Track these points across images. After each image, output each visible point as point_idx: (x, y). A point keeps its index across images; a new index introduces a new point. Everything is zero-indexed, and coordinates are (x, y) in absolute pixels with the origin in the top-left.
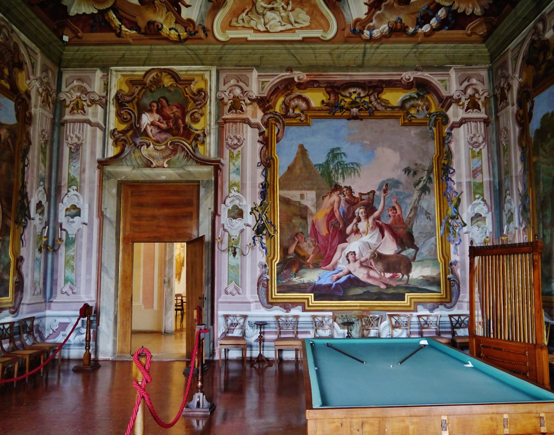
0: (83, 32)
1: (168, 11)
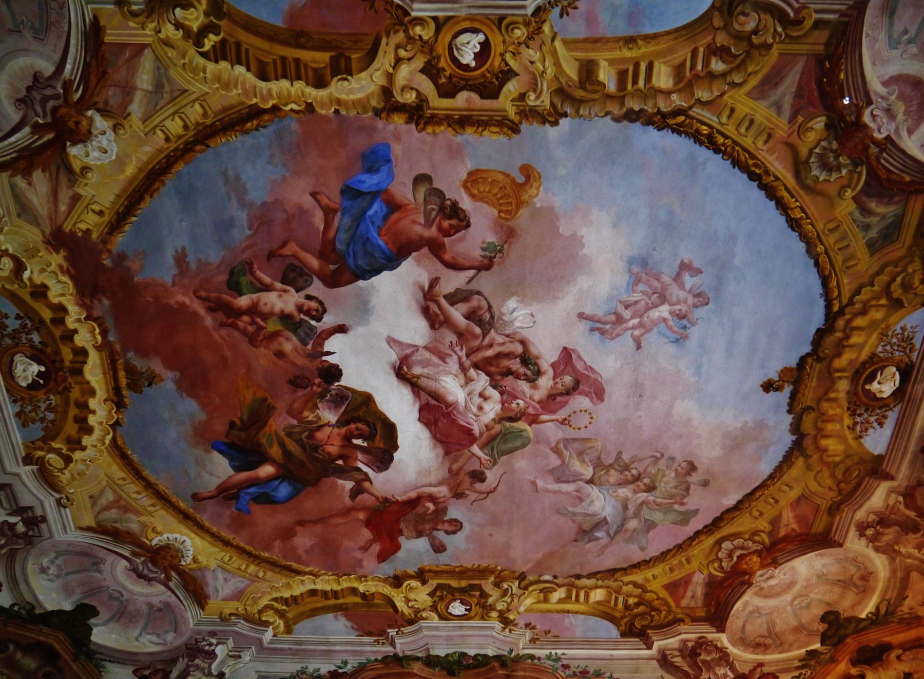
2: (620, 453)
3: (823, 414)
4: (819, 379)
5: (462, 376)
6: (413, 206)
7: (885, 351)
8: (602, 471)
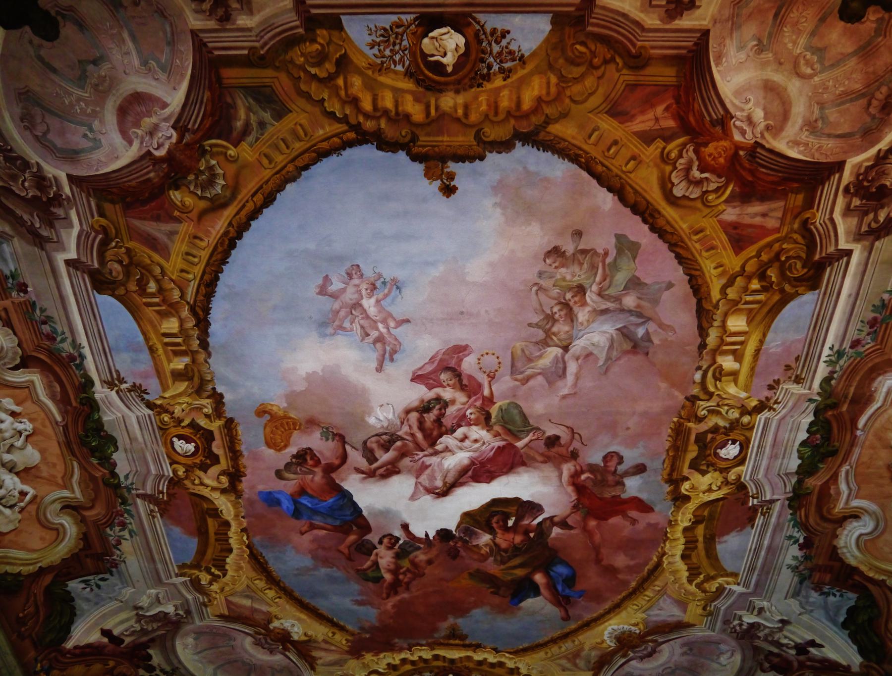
2: (530, 325)
3: (487, 116)
4: (440, 133)
5: (443, 454)
6: (300, 481)
7: (402, 61)
8: (552, 339)
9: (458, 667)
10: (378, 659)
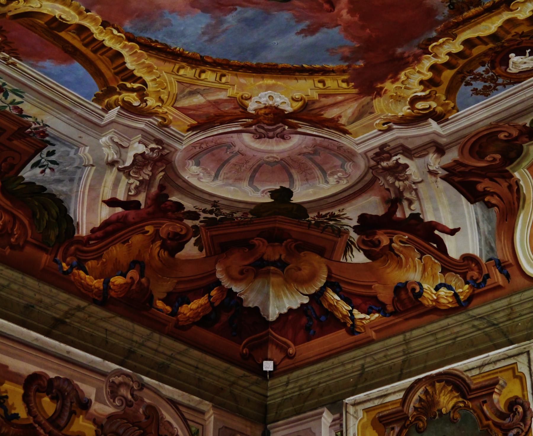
0: (295, 345)
1: (422, 254)
9: (509, 41)
10: (403, 82)
